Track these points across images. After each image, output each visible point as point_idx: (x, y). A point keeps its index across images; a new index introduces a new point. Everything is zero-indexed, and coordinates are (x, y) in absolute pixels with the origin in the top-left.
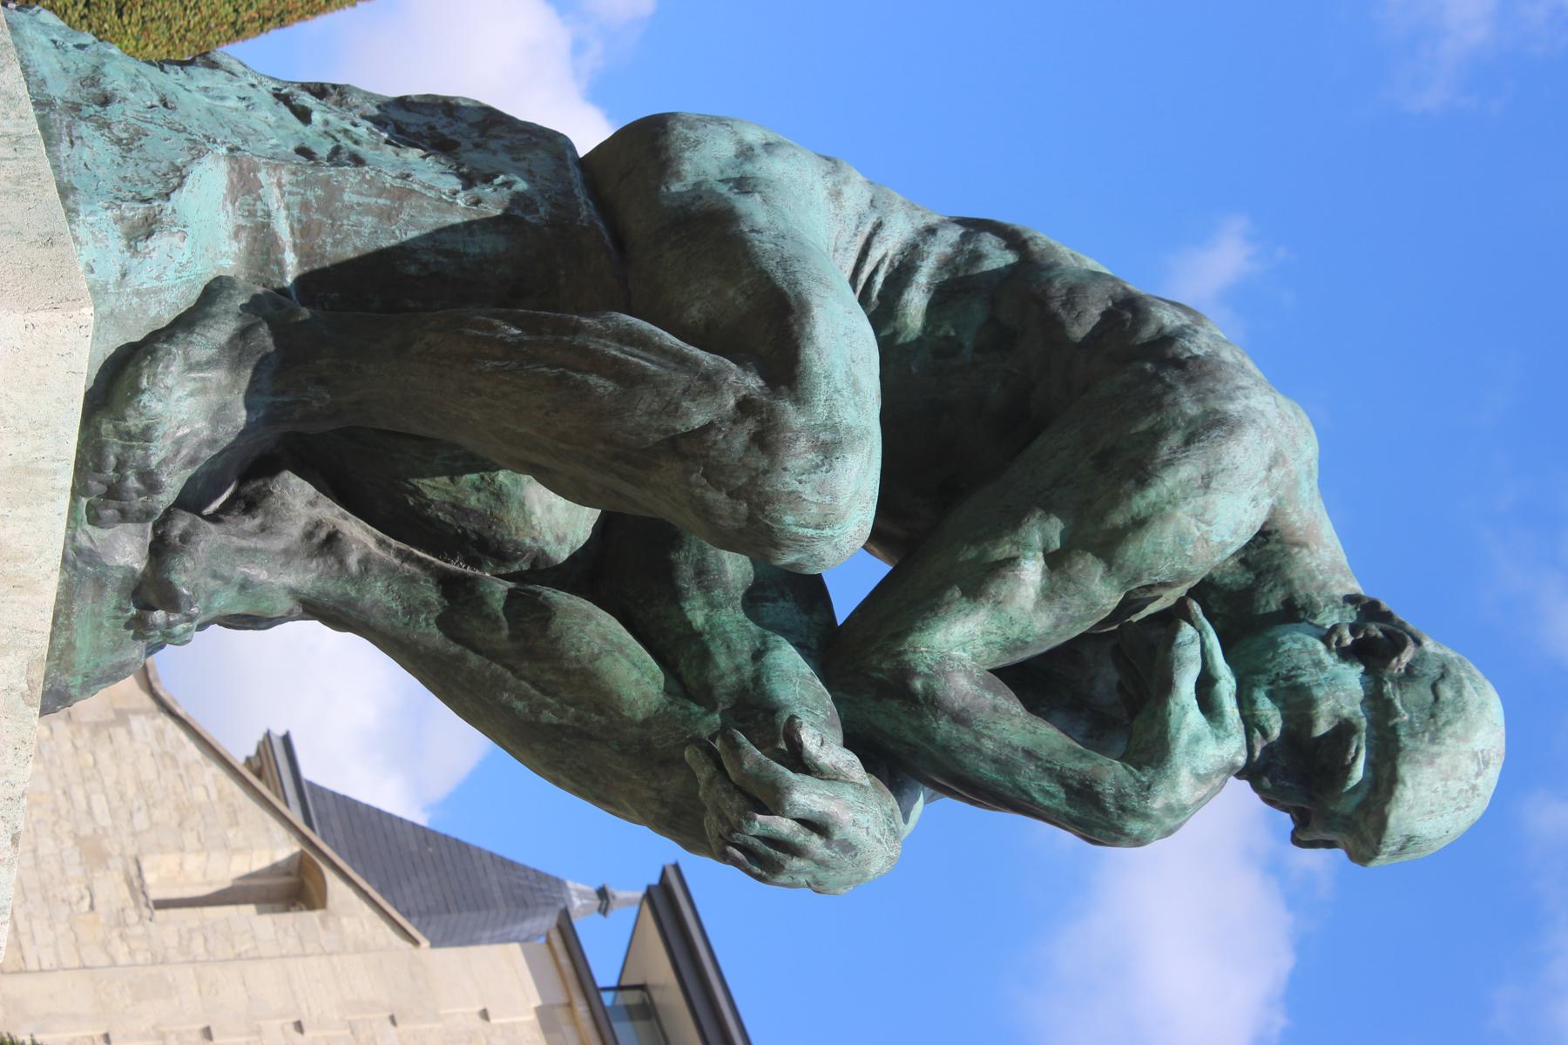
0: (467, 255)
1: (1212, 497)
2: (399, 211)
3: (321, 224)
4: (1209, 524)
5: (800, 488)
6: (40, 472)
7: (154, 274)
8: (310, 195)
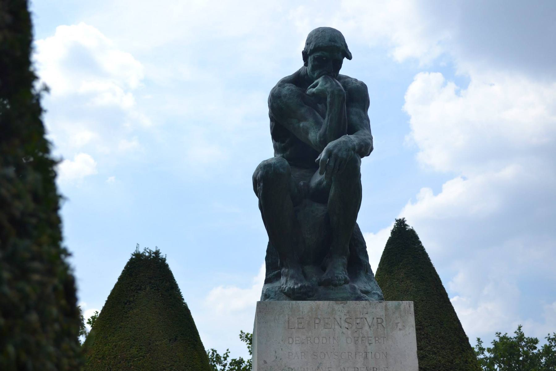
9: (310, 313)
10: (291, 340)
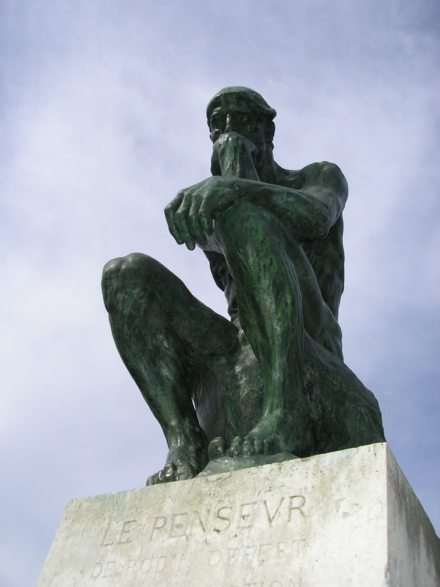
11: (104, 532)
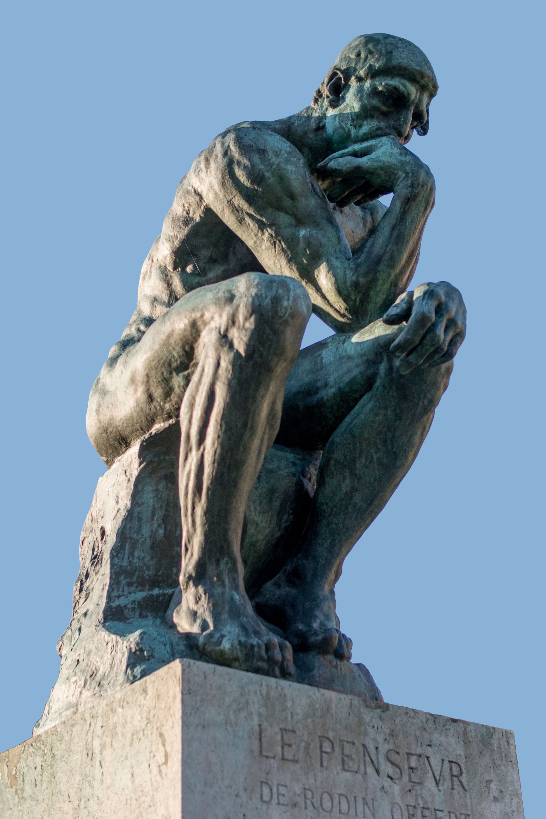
0: (154, 506)
1: (268, 149)
2: (131, 539)
3: (139, 577)
4: (281, 150)
5: (269, 298)
6: (268, 693)
7: (163, 647)
8: (124, 582)
9: (309, 720)
10: (266, 791)
11: (257, 735)
